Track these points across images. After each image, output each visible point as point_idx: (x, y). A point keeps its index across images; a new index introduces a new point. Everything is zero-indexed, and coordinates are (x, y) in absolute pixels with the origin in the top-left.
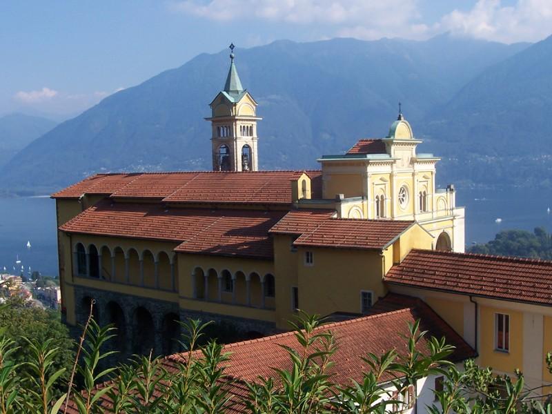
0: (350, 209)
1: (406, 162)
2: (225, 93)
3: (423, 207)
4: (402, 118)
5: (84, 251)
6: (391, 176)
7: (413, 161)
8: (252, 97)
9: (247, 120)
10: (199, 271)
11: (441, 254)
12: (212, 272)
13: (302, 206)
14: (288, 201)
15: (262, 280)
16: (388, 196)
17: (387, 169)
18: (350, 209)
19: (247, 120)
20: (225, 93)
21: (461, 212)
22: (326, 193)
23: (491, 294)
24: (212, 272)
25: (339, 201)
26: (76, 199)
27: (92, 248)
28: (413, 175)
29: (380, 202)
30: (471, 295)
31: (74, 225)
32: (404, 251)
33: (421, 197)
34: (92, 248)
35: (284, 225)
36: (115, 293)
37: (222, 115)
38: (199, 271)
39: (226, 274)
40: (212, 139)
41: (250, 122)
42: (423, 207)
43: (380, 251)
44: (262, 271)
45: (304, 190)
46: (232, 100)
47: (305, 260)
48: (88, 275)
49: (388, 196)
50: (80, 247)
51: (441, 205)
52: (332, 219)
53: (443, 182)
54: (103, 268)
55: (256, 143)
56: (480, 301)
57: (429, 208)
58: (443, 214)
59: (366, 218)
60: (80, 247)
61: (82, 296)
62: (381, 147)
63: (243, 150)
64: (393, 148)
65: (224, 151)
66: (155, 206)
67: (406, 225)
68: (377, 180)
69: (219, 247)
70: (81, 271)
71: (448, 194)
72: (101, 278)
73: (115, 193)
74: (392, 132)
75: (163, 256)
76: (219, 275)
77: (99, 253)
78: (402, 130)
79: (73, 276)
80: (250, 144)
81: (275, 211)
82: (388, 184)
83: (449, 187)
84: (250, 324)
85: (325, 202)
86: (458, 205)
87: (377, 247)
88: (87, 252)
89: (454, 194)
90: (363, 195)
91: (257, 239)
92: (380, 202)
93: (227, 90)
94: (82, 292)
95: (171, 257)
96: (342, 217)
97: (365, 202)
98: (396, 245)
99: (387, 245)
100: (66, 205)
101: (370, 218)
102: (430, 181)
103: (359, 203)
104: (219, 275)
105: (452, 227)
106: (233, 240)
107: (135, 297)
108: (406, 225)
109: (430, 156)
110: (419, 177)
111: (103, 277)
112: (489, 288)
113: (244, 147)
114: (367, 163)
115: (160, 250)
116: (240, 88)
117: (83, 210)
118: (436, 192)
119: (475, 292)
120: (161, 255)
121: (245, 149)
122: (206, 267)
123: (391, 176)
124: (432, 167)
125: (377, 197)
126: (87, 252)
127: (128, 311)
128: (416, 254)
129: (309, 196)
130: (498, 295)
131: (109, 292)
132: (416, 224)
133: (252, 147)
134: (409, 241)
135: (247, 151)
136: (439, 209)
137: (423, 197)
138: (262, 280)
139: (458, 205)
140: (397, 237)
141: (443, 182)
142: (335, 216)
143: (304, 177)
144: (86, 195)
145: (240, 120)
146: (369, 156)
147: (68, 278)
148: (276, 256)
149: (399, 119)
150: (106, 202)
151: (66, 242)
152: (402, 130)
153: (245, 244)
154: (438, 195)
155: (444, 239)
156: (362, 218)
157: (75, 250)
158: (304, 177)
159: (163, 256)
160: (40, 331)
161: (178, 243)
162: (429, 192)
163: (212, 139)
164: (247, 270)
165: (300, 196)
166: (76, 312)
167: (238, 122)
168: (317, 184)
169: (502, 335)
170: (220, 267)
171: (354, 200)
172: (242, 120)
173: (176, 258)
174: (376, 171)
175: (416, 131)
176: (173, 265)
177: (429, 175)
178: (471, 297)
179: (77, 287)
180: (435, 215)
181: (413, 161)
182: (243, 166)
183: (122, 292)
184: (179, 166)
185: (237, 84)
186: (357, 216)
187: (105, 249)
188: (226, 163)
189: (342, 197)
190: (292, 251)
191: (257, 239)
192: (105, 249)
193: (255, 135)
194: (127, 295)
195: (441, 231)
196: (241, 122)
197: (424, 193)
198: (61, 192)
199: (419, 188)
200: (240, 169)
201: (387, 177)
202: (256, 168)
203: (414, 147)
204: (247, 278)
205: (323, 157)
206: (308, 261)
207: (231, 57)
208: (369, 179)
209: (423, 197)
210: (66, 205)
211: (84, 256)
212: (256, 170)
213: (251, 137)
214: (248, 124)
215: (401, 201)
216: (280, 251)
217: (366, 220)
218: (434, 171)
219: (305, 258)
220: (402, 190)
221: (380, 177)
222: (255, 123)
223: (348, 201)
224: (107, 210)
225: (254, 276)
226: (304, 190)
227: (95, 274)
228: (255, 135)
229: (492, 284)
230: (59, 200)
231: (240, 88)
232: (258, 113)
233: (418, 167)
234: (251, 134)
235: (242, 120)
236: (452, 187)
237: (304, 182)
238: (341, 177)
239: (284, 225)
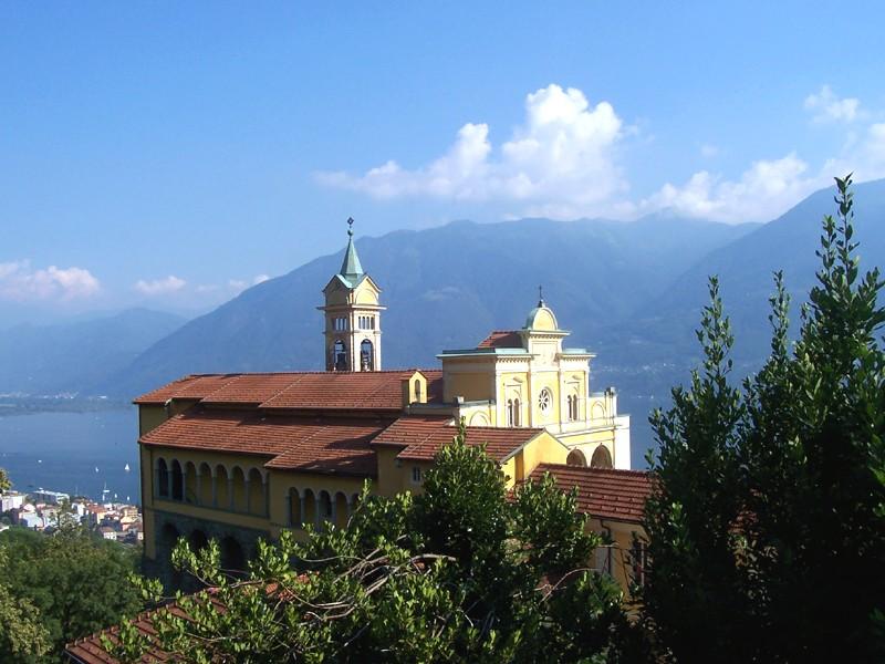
0: (474, 415)
1: (550, 358)
2: (341, 277)
3: (573, 414)
4: (543, 305)
7: (558, 358)
8: (377, 284)
9: (367, 310)
10: (293, 491)
11: (574, 469)
12: (309, 493)
13: (417, 412)
14: (396, 405)
17: (523, 366)
18: (474, 415)
19: (367, 310)
20: (341, 277)
21: (625, 421)
22: (447, 398)
23: (626, 517)
24: (309, 493)
25: (457, 405)
26: (161, 405)
27: (176, 464)
28: (559, 374)
29: (514, 407)
30: (602, 519)
31: (156, 437)
32: (530, 465)
33: (570, 402)
34: (176, 464)
35: (390, 435)
36: (200, 520)
37: (337, 302)
38: (293, 491)
39: (325, 495)
40: (325, 333)
42: (573, 414)
45: (417, 393)
46: (349, 285)
47: (412, 478)
48: (170, 497)
50: (162, 462)
51: (598, 412)
52: (447, 427)
53: (598, 385)
56: (614, 525)
57: (581, 414)
58: (601, 423)
59: (494, 425)
60: (162, 462)
62: (516, 340)
63: (362, 347)
64: (530, 340)
65: (339, 347)
66: (249, 413)
67: (532, 433)
69: (318, 462)
70: (163, 493)
73: (208, 398)
74: (530, 322)
75: (255, 473)
76: (317, 497)
77: (183, 471)
78: (543, 319)
79: (153, 498)
80: (372, 338)
81: (384, 418)
82: (525, 385)
83: (609, 390)
85: (442, 403)
86: (621, 412)
88: (169, 469)
89: (615, 398)
90: (489, 397)
91: (363, 452)
92: (514, 407)
93: (344, 273)
95: (263, 473)
97: (493, 407)
98: (519, 457)
99: (506, 458)
100: (151, 411)
101: (499, 426)
102: (582, 382)
103: (485, 408)
104: (317, 497)
105: (613, 440)
106: (334, 455)
107: (220, 523)
108: (532, 433)
109: (581, 351)
110: (566, 377)
112: (624, 510)
113: (363, 342)
114: (495, 359)
115: (251, 466)
116: (359, 270)
117: (170, 417)
118: (590, 396)
119: (607, 514)
120: (250, 472)
122: (301, 486)
123: (528, 375)
124: (584, 365)
125: (510, 401)
126: (169, 469)
129: (424, 399)
130: (634, 518)
131: (191, 519)
133: (373, 341)
134: (536, 454)
135: (367, 347)
137: (573, 402)
139: (621, 412)
140: (519, 449)
141: (598, 385)
142: (453, 424)
143: (417, 376)
144: (173, 399)
145: (358, 309)
146: (499, 351)
147: (148, 503)
148: (380, 472)
149: (540, 306)
150: (195, 408)
151: (147, 453)
152: (543, 319)
153: (348, 458)
154: (593, 400)
155: (602, 454)
156: (489, 425)
157: (156, 466)
158: (417, 376)
159: (255, 473)
160: (95, 563)
161: (274, 456)
162: (581, 396)
163: (325, 333)
165: (413, 399)
166: (157, 543)
167: (355, 312)
168: (435, 388)
169: (174, 488)
170: (317, 487)
171: (478, 404)
172: (361, 309)
173: (268, 475)
174: (507, 371)
175: (562, 320)
177: (581, 375)
178: (601, 521)
179: (158, 513)
180: (590, 424)
181: (558, 358)
182: (362, 366)
183: (208, 518)
184: (292, 369)
185: (356, 266)
186: (483, 424)
187: (190, 465)
188: (343, 362)
189: (461, 400)
190: (399, 466)
191: (363, 452)
192: (190, 465)
193: (377, 328)
195: (598, 444)
198: (149, 395)
199: (568, 390)
200: (358, 369)
201: (523, 377)
202: (378, 367)
203: (560, 340)
205: (445, 352)
206: (415, 479)
207: (350, 233)
208: (497, 378)
209: (573, 402)
210: (151, 411)
211: (168, 478)
212: (379, 369)
216: (385, 466)
217: (492, 428)
218: (588, 370)
219: (412, 474)
220: (545, 393)
221: (514, 376)
222: (378, 313)
223: (469, 406)
224: (193, 418)
226: (417, 393)
227: (178, 496)
228: (377, 328)
229: (628, 505)
230: (143, 406)
231: (359, 270)
232: (382, 301)
234: (373, 327)
235: (361, 309)
236: (612, 390)
237: (417, 382)
238: (467, 375)
239: (390, 435)
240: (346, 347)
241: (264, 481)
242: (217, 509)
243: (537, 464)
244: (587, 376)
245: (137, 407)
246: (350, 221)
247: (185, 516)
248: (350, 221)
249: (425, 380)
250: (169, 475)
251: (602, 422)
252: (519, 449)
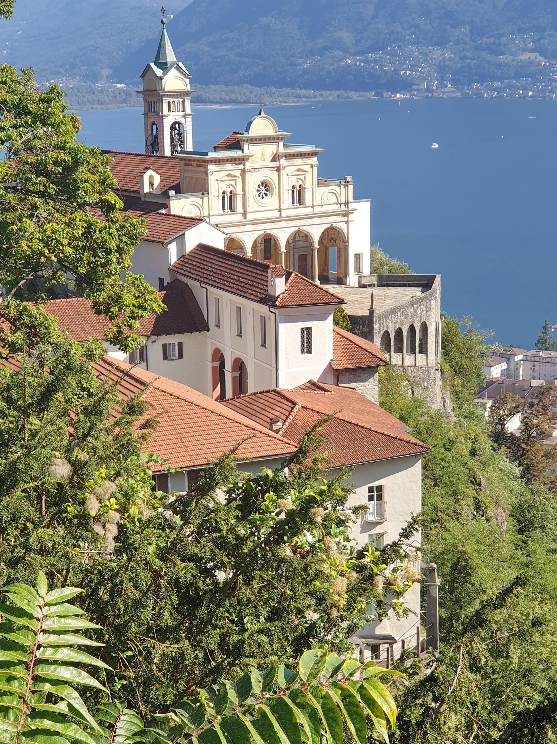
2: (152, 65)
4: (263, 113)
6: (243, 172)
32: (190, 246)
43: (163, 244)
49: (239, 190)
53: (325, 176)
55: (189, 119)
57: (308, 201)
71: (342, 187)
80: (182, 120)
82: (239, 181)
86: (357, 197)
89: (351, 188)
96: (172, 213)
123: (243, 172)
141: (325, 176)
142: (163, 211)
149: (260, 114)
158: (150, 172)
177: (308, 168)
180: (317, 209)
237: (151, 177)
240: (160, 129)
244: (315, 169)
249: (159, 176)
251: (335, 207)
252: (183, 233)
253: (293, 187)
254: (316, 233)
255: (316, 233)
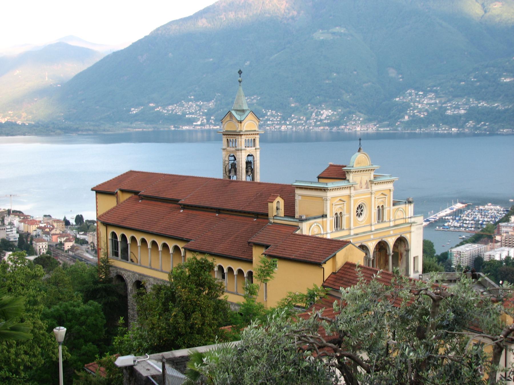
5: (117, 238)
15: (245, 275)
16: (344, 213)
17: (346, 192)
27: (123, 237)
34: (123, 237)
36: (140, 275)
41: (254, 136)
44: (246, 269)
50: (114, 235)
54: (131, 252)
55: (258, 152)
57: (386, 218)
60: (114, 235)
61: (115, 275)
68: (336, 201)
72: (129, 261)
73: (143, 192)
77: (129, 242)
84: (237, 308)
87: (318, 261)
88: (119, 239)
94: (115, 271)
95: (182, 251)
107: (155, 279)
111: (131, 260)
118: (394, 205)
121: (249, 157)
123: (350, 196)
125: (336, 214)
126: (119, 239)
127: (149, 288)
128: (348, 266)
131: (134, 273)
132: (350, 245)
135: (250, 159)
136: (397, 218)
137: (380, 210)
138: (245, 275)
142: (298, 232)
148: (254, 259)
157: (110, 237)
164: (236, 267)
167: (243, 137)
176: (184, 256)
180: (392, 224)
187: (133, 239)
192: (133, 239)
194: (149, 277)
195: (399, 236)
196: (246, 136)
197: (382, 206)
204: (235, 273)
209: (380, 210)
213: (254, 148)
214: (251, 137)
215: (359, 215)
221: (339, 199)
222: (258, 136)
225: (240, 272)
228: (258, 146)
233: (375, 188)
234: (254, 146)
237: (278, 202)
241: (182, 255)
242: (151, 268)
243: (344, 263)
244: (392, 193)
245: (95, 192)
246: (240, 72)
247: (129, 271)
248: (240, 72)
250: (119, 243)
252: (334, 254)
253: (378, 207)
254: (391, 242)
255: (391, 242)
